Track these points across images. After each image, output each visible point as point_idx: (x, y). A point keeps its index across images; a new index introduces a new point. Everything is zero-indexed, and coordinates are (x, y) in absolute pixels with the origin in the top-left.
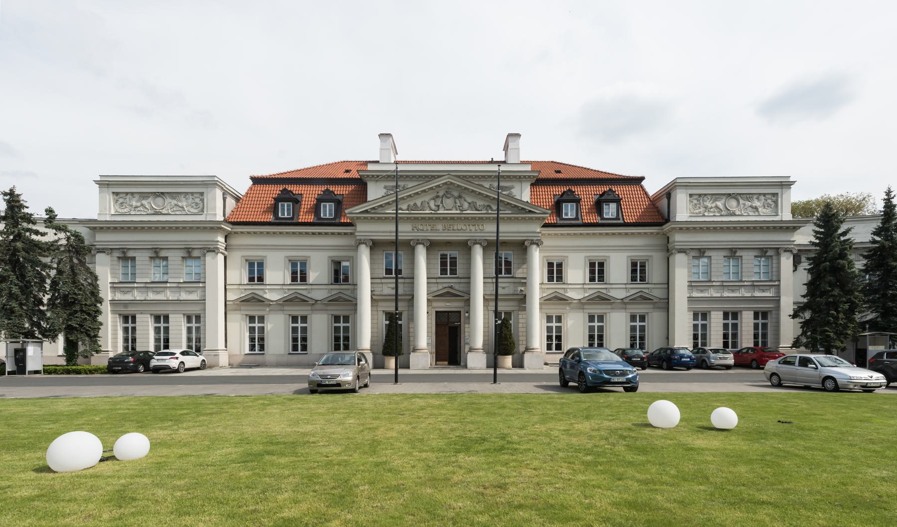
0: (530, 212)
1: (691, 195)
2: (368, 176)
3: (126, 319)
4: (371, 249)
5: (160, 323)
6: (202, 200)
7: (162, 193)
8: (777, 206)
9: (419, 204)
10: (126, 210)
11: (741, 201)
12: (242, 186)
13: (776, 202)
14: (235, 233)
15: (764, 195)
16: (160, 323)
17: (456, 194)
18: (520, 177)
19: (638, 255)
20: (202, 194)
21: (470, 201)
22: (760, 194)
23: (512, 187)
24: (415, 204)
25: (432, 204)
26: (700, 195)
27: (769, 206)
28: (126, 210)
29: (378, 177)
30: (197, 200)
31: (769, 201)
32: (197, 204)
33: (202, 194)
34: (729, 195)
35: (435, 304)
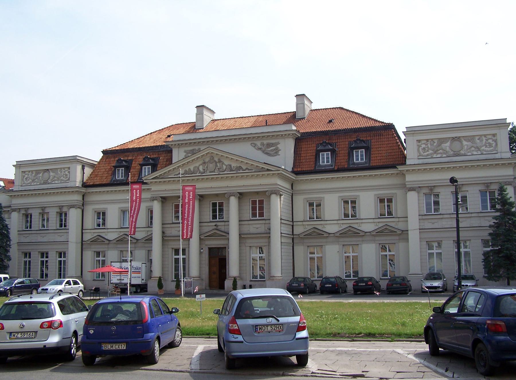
0: (268, 170)
1: (419, 141)
2: (172, 145)
3: (26, 255)
4: (163, 202)
5: (99, 257)
6: (69, 172)
7: (48, 170)
8: (497, 145)
9: (192, 169)
10: (28, 182)
11: (465, 143)
12: (97, 157)
13: (496, 141)
14: (89, 192)
15: (485, 136)
16: (99, 257)
17: (216, 159)
18: (282, 135)
19: (385, 193)
20: (69, 168)
21: (227, 164)
22: (481, 136)
23: (278, 143)
24: (190, 169)
25: (201, 168)
26: (427, 140)
27: (490, 145)
28: (28, 182)
29: (180, 144)
30: (67, 173)
31: (490, 141)
32: (66, 175)
33: (69, 168)
34: (454, 139)
35: (208, 243)
